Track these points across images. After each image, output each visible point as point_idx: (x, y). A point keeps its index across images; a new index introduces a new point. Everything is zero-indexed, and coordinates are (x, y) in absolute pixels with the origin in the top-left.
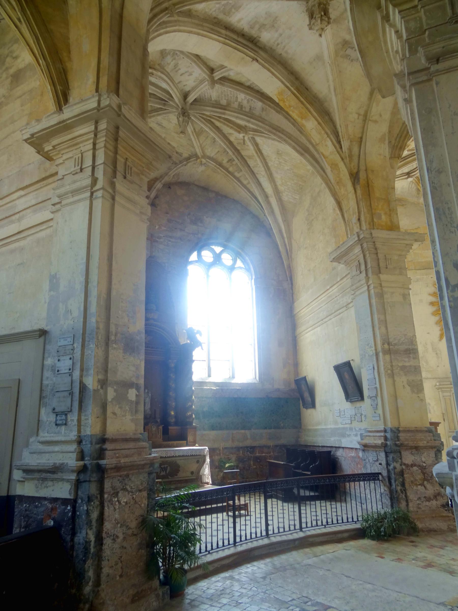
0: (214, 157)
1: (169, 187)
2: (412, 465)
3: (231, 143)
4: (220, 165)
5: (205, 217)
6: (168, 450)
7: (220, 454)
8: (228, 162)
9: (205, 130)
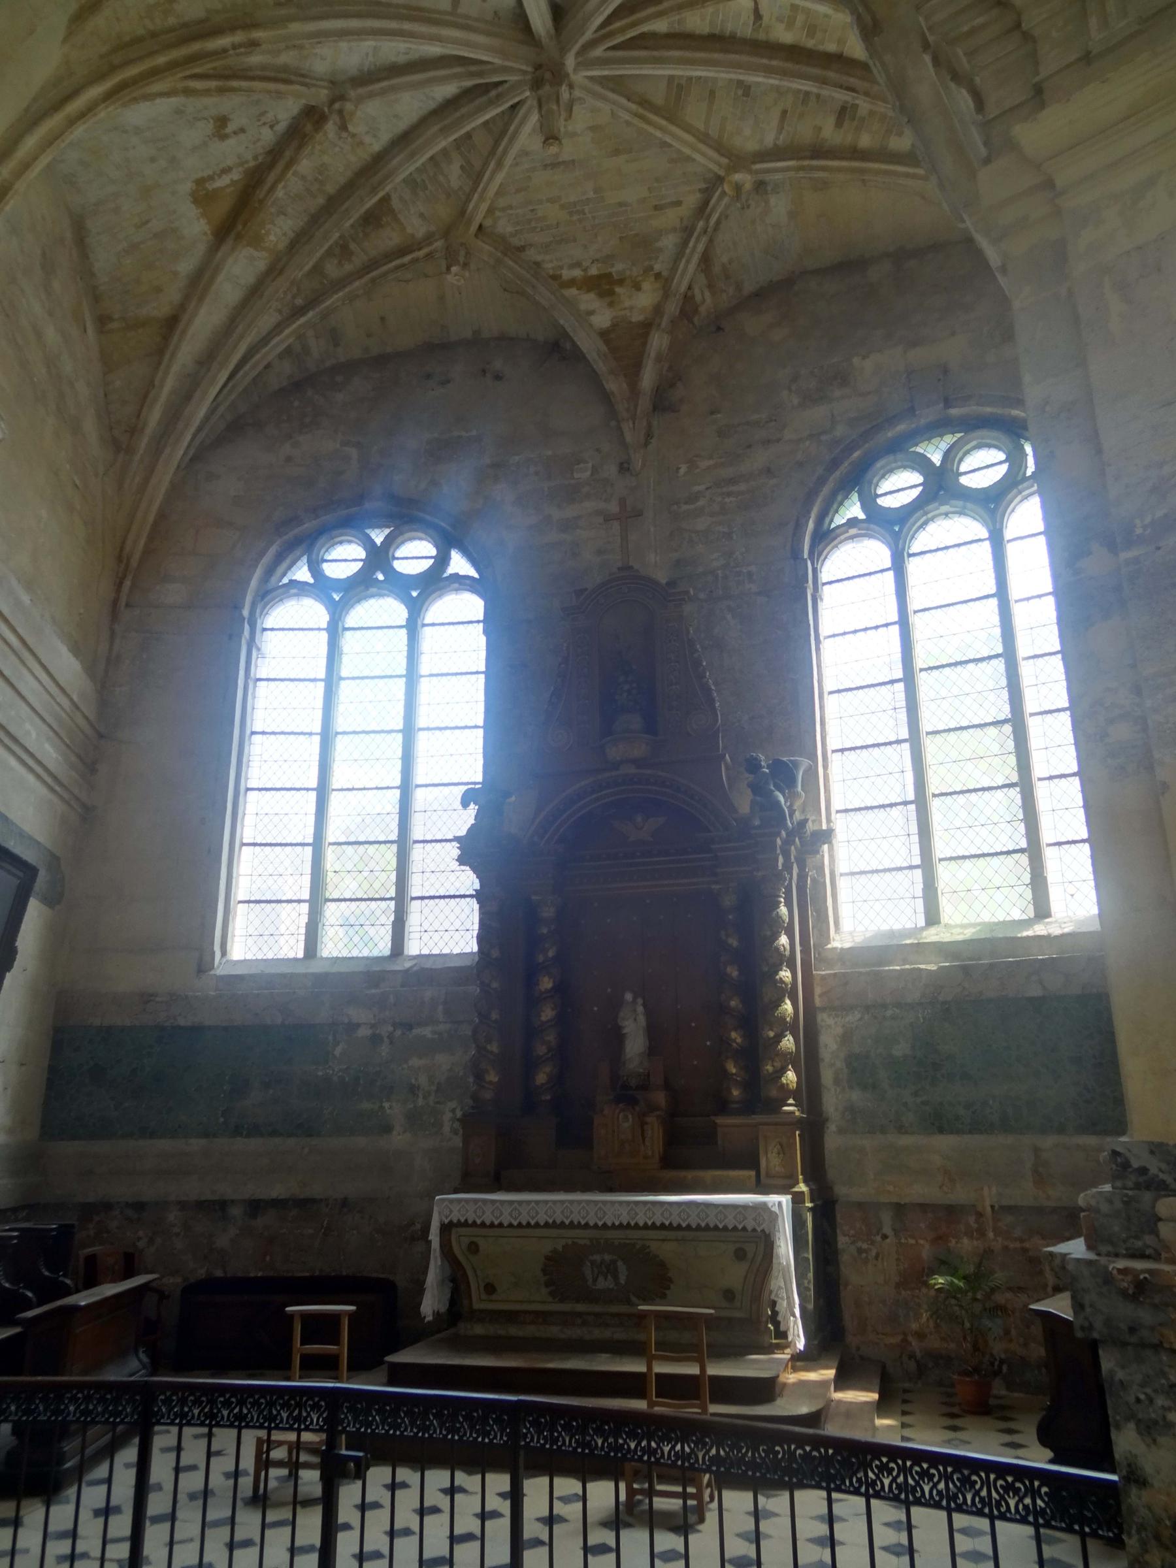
0: (780, 142)
1: (719, 329)
3: (794, 53)
4: (819, 151)
5: (856, 360)
6: (605, 1203)
7: (982, 1233)
8: (839, 123)
9: (690, 79)
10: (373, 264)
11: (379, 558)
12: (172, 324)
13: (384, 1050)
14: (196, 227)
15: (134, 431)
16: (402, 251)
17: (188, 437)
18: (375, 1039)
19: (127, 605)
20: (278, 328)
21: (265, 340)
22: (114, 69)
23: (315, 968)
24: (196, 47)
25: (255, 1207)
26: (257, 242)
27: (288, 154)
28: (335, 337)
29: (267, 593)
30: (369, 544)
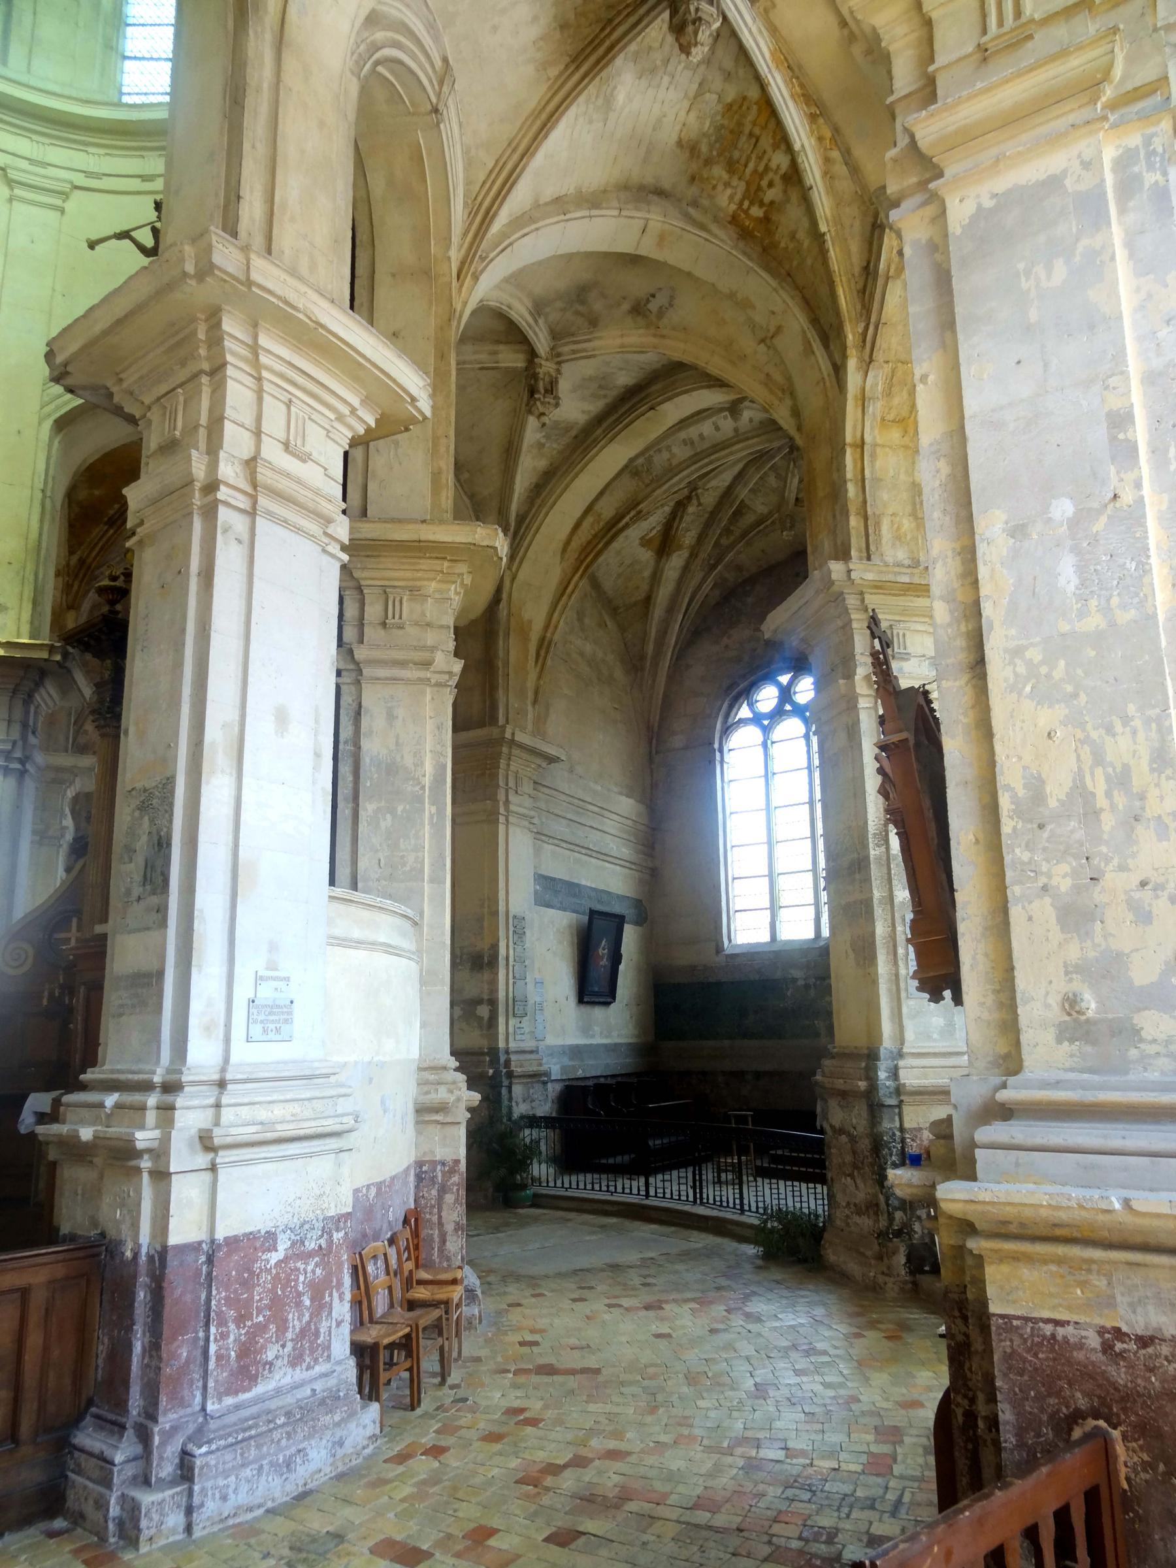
2: (841, 1131)
10: (744, 535)
11: (786, 694)
12: (648, 600)
13: (812, 992)
14: (646, 556)
15: (642, 657)
16: (759, 523)
17: (669, 654)
18: (807, 987)
19: (657, 753)
20: (704, 580)
21: (699, 587)
22: (582, 562)
23: (775, 948)
24: (614, 530)
25: (758, 1075)
26: (680, 548)
27: (679, 514)
28: (739, 568)
29: (727, 729)
30: (779, 685)
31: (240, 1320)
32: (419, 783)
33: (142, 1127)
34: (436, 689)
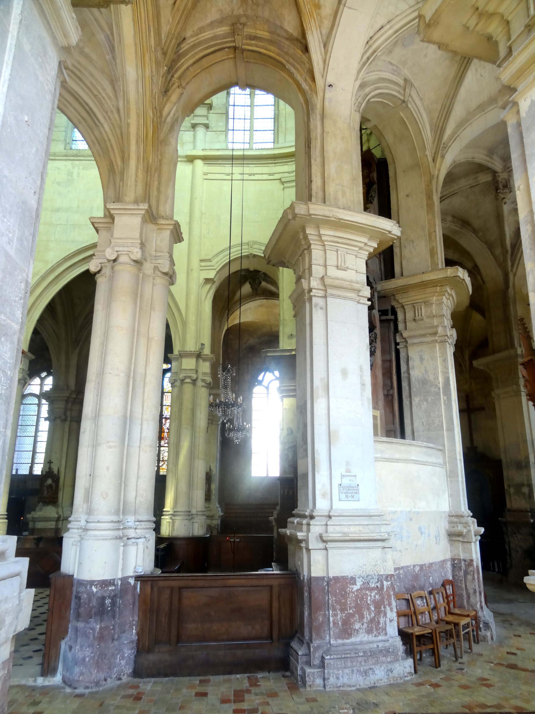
31: (342, 610)
32: (437, 387)
33: (301, 531)
34: (441, 344)
